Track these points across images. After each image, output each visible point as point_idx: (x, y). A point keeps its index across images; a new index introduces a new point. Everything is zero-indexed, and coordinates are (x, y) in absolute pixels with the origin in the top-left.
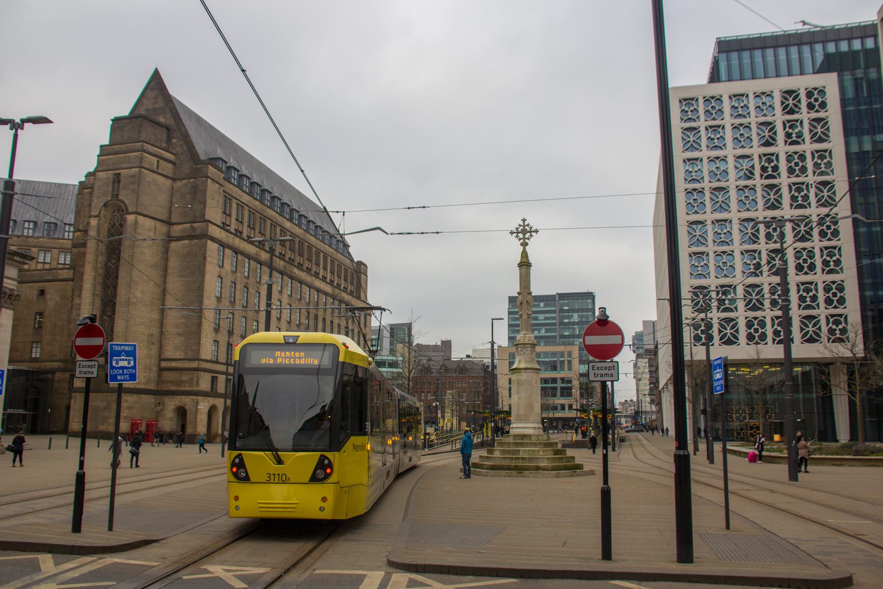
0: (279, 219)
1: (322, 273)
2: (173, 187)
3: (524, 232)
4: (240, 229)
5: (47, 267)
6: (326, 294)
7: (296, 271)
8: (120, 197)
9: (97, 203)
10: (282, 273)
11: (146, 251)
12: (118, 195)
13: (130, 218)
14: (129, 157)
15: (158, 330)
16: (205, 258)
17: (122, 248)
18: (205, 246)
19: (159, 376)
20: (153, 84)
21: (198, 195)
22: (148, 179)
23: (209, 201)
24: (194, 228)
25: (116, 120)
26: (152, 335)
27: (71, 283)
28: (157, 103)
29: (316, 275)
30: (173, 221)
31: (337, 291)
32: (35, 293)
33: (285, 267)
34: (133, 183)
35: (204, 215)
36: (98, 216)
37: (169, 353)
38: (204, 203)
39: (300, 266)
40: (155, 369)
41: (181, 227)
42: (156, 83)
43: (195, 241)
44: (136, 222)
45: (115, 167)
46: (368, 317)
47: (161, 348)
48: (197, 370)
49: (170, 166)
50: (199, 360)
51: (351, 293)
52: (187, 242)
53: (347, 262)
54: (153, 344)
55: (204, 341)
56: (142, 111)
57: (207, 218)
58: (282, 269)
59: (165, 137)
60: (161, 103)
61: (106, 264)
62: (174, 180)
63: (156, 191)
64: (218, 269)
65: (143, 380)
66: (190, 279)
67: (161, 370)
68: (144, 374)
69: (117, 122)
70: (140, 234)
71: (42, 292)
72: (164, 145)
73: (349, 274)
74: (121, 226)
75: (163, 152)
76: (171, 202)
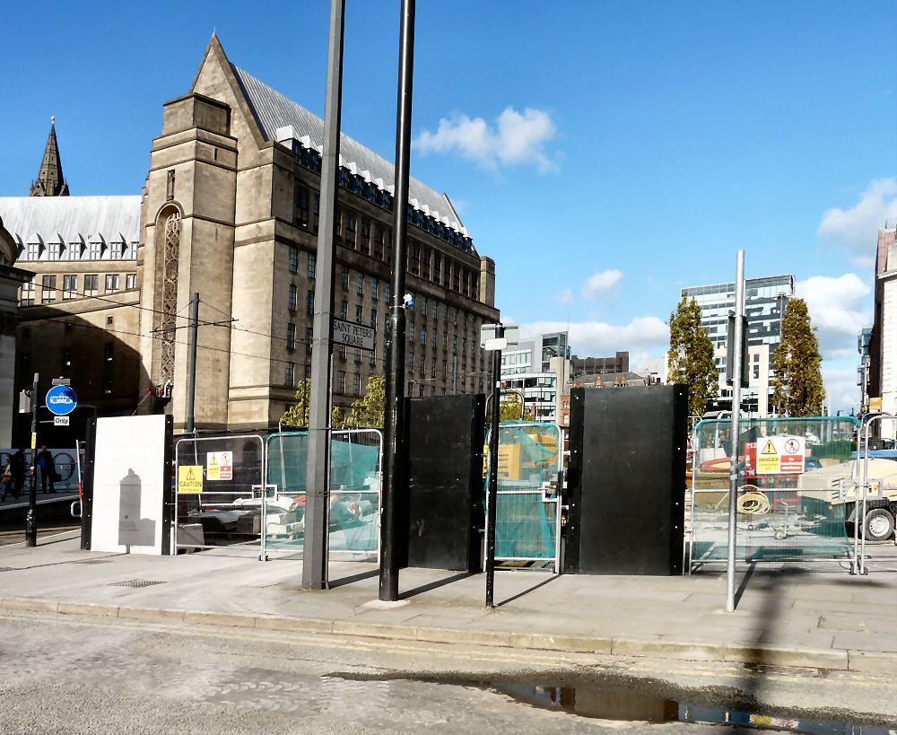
8: (175, 199)
11: (206, 261)
12: (173, 197)
14: (183, 149)
17: (180, 260)
22: (205, 173)
26: (218, 361)
28: (214, 78)
45: (169, 163)
52: (253, 245)
64: (291, 276)
65: (209, 414)
66: (257, 291)
68: (211, 406)
70: (199, 241)
74: (178, 232)
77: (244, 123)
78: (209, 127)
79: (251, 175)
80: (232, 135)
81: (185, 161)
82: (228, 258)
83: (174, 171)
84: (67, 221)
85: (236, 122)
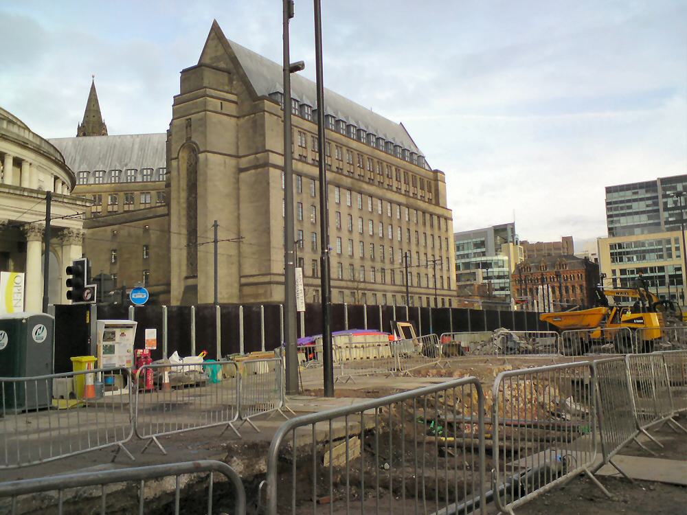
0: (344, 140)
1: (395, 184)
2: (237, 125)
3: (93, 77)
4: (304, 155)
5: (148, 206)
6: (399, 204)
7: (365, 186)
8: (192, 139)
9: (176, 147)
10: (350, 189)
12: (190, 138)
13: (201, 156)
15: (237, 251)
16: (268, 184)
17: (198, 183)
18: (268, 173)
19: (240, 291)
20: (213, 34)
21: (258, 129)
23: (268, 133)
24: (257, 159)
25: (184, 72)
27: (167, 217)
28: (217, 51)
29: (390, 188)
30: (241, 154)
31: (412, 200)
32: (140, 231)
33: (352, 184)
34: (201, 126)
35: (264, 146)
36: (177, 158)
37: (248, 270)
38: (263, 135)
39: (371, 182)
40: (236, 285)
41: (247, 158)
42: (216, 33)
43: (260, 170)
44: (206, 159)
45: (186, 114)
46: (449, 222)
47: (240, 266)
48: (269, 283)
49: (233, 105)
50: (270, 274)
51: (430, 201)
52: (253, 171)
53: (422, 171)
54: (232, 264)
55: (273, 257)
56: (207, 61)
57: (267, 148)
58: (349, 185)
59: (226, 80)
60: (221, 51)
61: (188, 199)
62: (238, 117)
63: (222, 130)
65: (226, 296)
67: (242, 285)
69: (186, 74)
71: (146, 231)
72: (226, 88)
73: (426, 183)
74: (196, 163)
75: (225, 94)
76: (237, 137)
77: (241, 83)
78: (214, 87)
79: (248, 120)
80: (233, 92)
81: (198, 112)
82: (234, 180)
83: (190, 119)
84: (108, 155)
85: (234, 83)
